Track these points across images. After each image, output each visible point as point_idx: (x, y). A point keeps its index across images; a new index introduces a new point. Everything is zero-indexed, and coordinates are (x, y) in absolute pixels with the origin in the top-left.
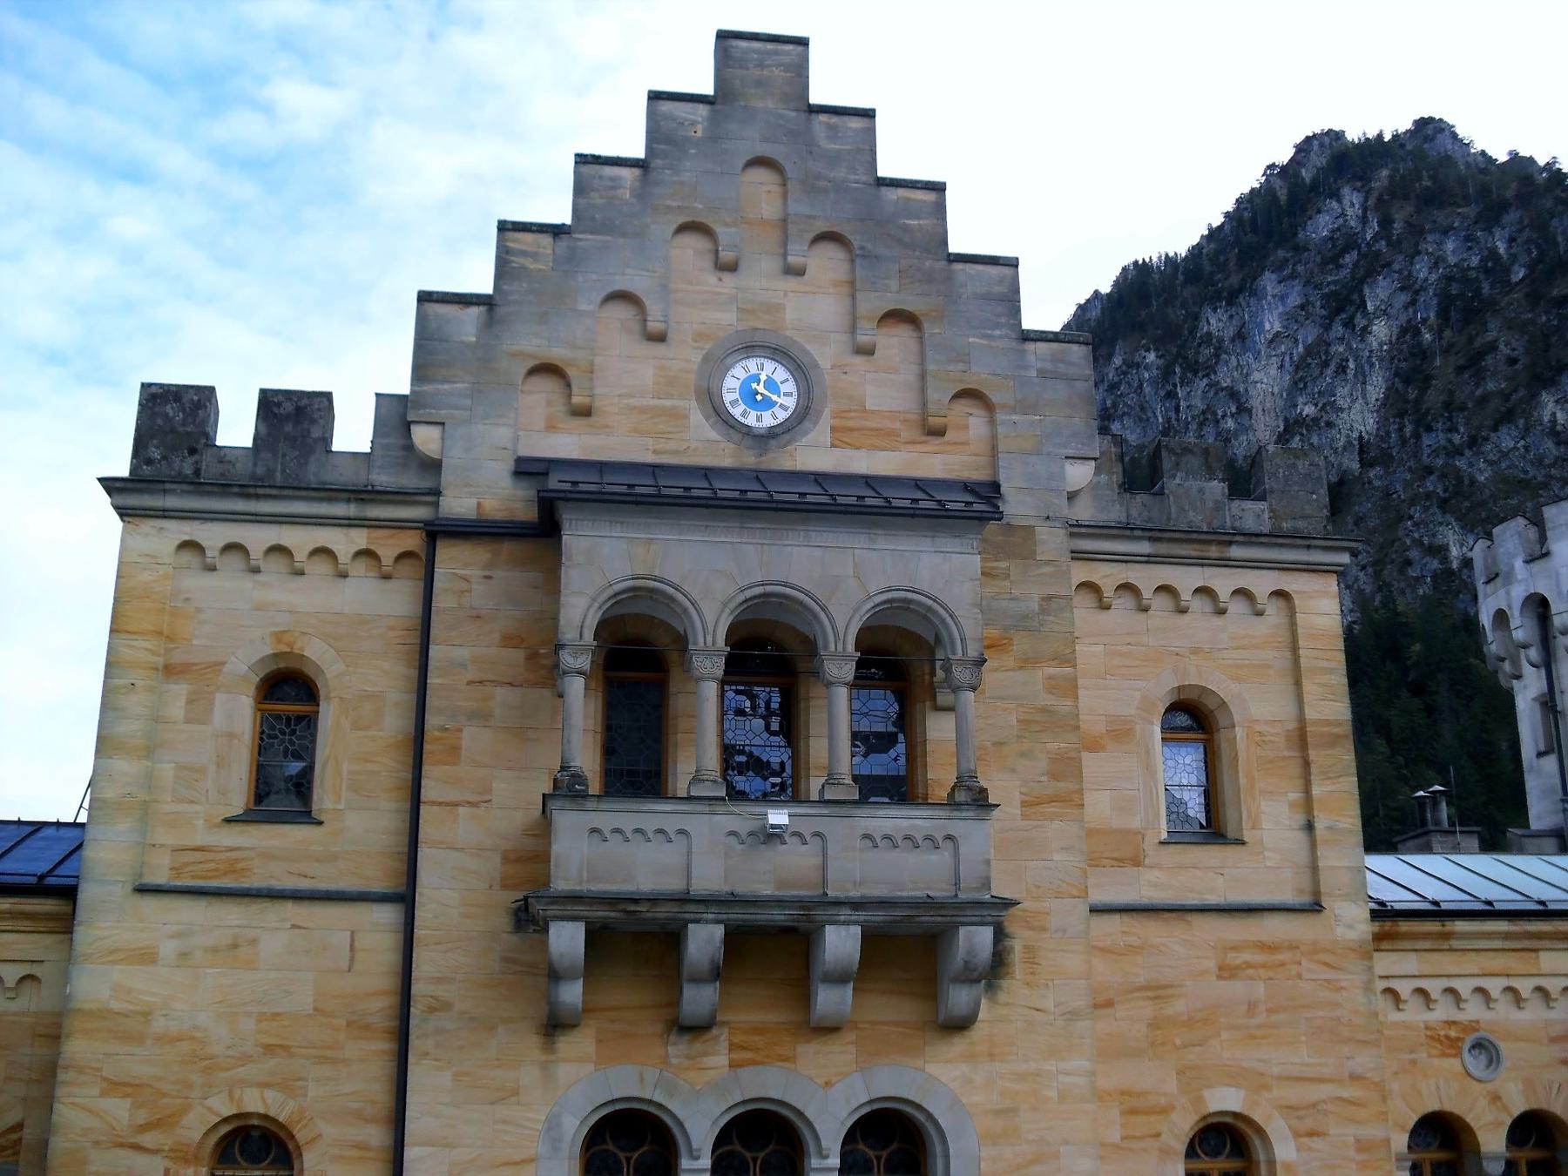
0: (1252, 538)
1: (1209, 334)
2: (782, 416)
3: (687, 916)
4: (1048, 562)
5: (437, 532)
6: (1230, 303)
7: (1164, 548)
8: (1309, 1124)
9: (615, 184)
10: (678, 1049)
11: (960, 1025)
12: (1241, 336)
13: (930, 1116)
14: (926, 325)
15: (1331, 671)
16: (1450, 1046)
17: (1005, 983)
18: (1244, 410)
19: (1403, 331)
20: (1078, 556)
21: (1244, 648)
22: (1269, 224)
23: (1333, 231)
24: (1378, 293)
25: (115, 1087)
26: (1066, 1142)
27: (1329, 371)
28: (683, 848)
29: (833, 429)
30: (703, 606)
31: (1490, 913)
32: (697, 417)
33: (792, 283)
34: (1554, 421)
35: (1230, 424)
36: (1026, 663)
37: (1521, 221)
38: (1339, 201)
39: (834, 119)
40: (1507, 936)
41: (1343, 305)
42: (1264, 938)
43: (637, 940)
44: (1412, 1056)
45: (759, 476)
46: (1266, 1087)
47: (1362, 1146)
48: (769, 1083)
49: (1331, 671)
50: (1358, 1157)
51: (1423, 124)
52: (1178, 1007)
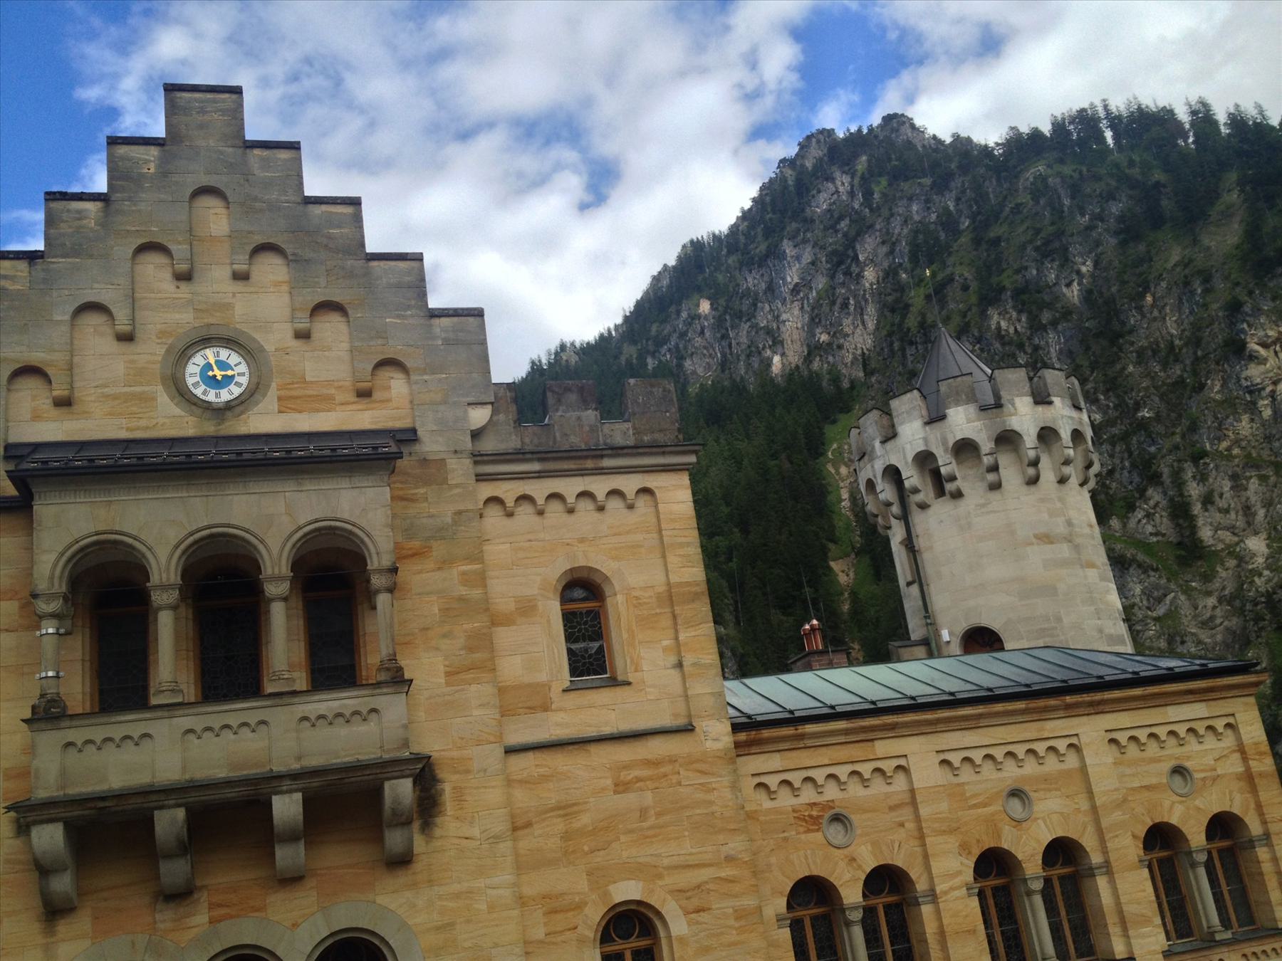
0: (617, 451)
1: (748, 289)
2: (237, 391)
3: (152, 805)
4: (457, 486)
8: (695, 902)
9: (81, 215)
10: (165, 917)
11: (402, 861)
12: (771, 289)
13: (382, 939)
14: (350, 312)
15: (688, 544)
16: (815, 820)
17: (438, 820)
20: (481, 478)
21: (620, 534)
24: (867, 247)
26: (496, 945)
27: (837, 308)
28: (177, 747)
29: (280, 399)
30: (269, 541)
31: (834, 715)
33: (239, 286)
34: (999, 328)
36: (444, 564)
39: (266, 153)
40: (846, 732)
41: (842, 261)
42: (650, 757)
44: (786, 834)
45: (217, 439)
46: (660, 876)
47: (740, 914)
49: (688, 544)
50: (737, 925)
52: (585, 820)
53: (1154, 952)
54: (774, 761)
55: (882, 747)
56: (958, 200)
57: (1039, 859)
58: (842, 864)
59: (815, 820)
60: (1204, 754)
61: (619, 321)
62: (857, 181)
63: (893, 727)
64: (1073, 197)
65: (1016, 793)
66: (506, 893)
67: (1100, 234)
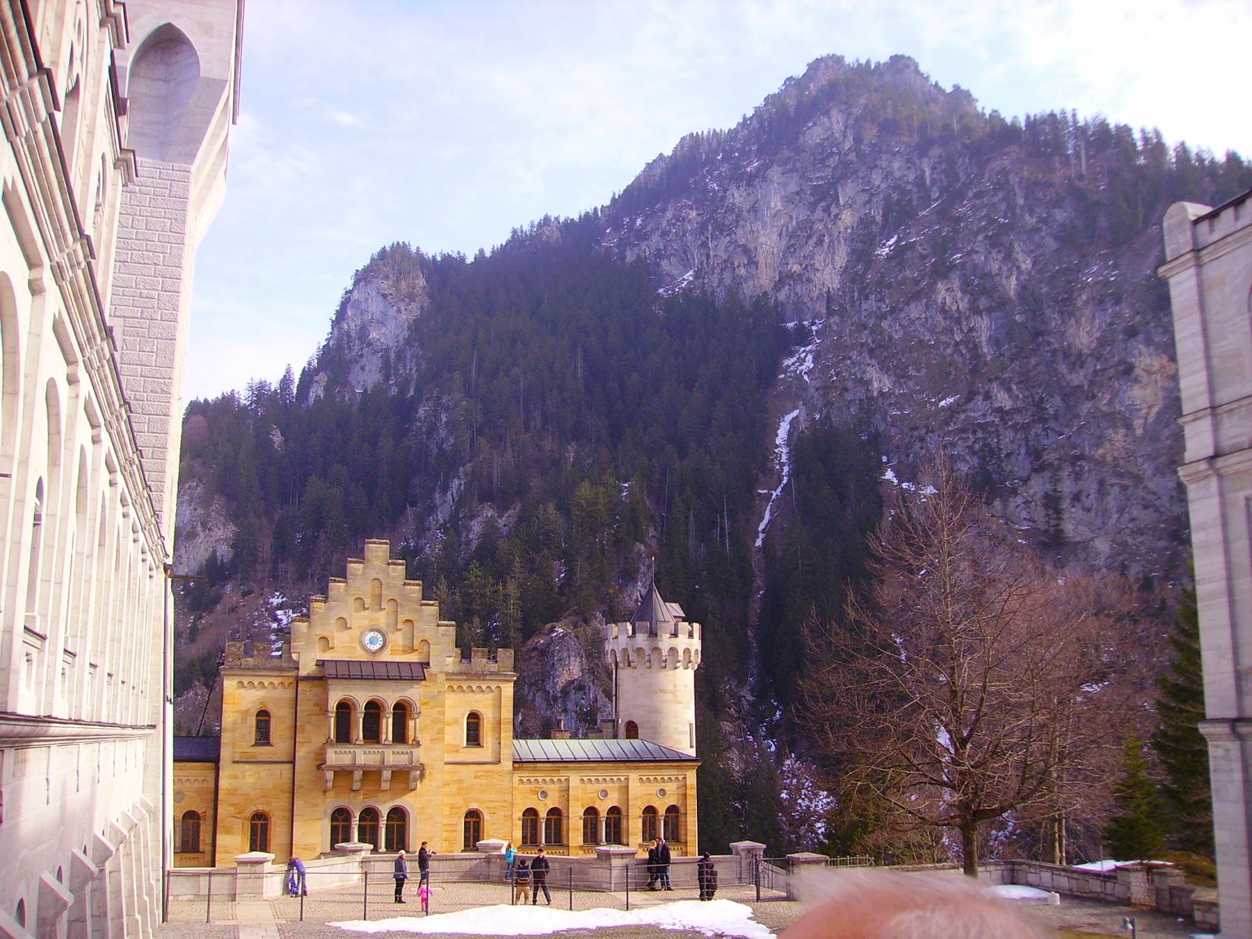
1: (733, 204)
5: (298, 680)
6: (748, 184)
10: (352, 795)
12: (754, 209)
18: (752, 263)
19: (861, 221)
22: (779, 127)
23: (824, 140)
24: (847, 192)
32: (359, 648)
35: (743, 271)
37: (940, 156)
38: (829, 118)
41: (825, 196)
43: (343, 773)
51: (896, 59)
54: (526, 774)
55: (562, 773)
56: (933, 169)
61: (607, 203)
62: (851, 122)
64: (1026, 198)
67: (1043, 238)
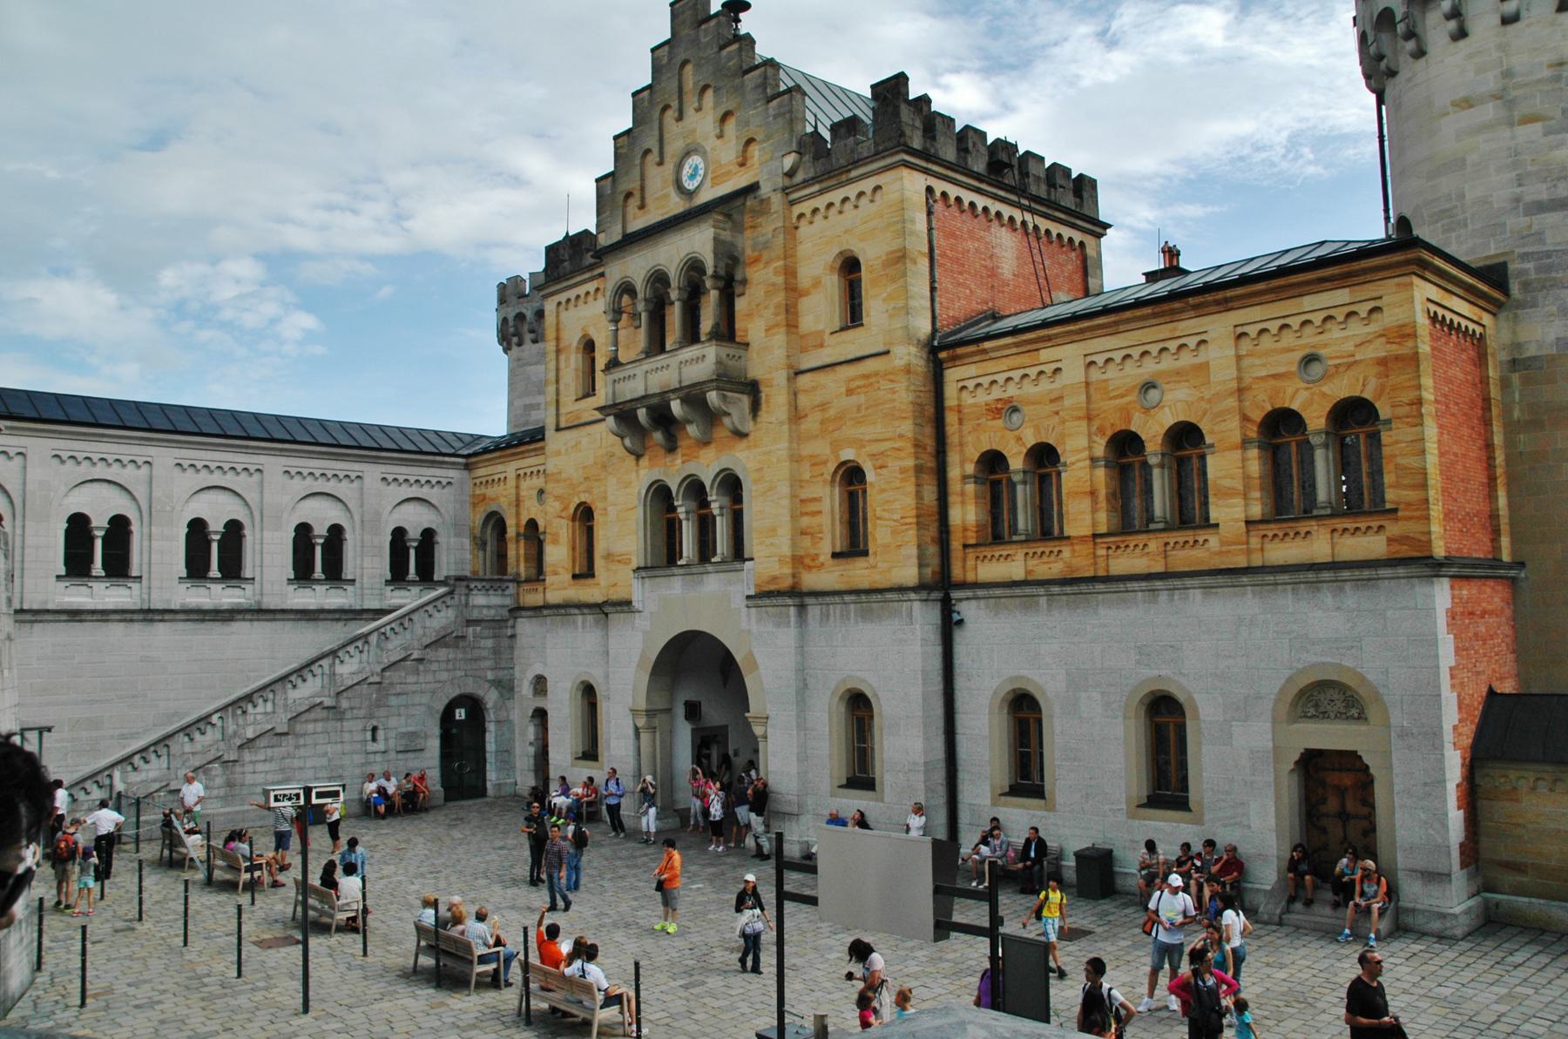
7: (824, 185)
8: (880, 462)
11: (740, 435)
25: (557, 498)
40: (1016, 345)
47: (903, 471)
48: (691, 468)
52: (832, 412)
53: (1237, 520)
54: (972, 370)
55: (1046, 354)
57: (1159, 439)
58: (1012, 442)
59: (999, 411)
60: (1339, 341)
63: (1049, 338)
65: (1149, 386)
66: (784, 454)
